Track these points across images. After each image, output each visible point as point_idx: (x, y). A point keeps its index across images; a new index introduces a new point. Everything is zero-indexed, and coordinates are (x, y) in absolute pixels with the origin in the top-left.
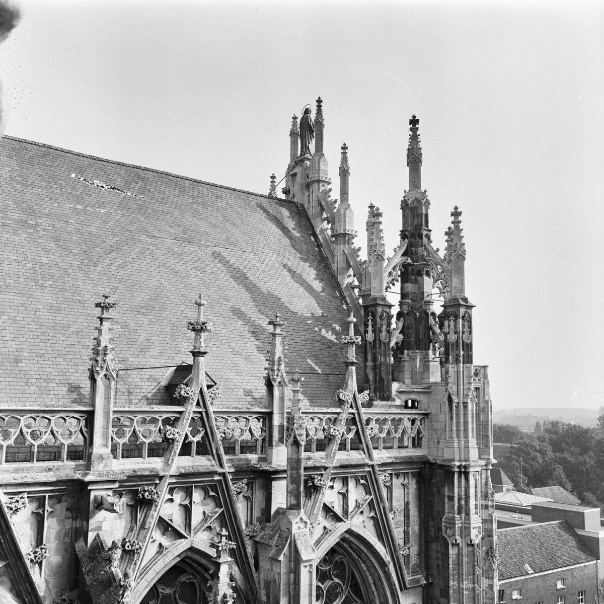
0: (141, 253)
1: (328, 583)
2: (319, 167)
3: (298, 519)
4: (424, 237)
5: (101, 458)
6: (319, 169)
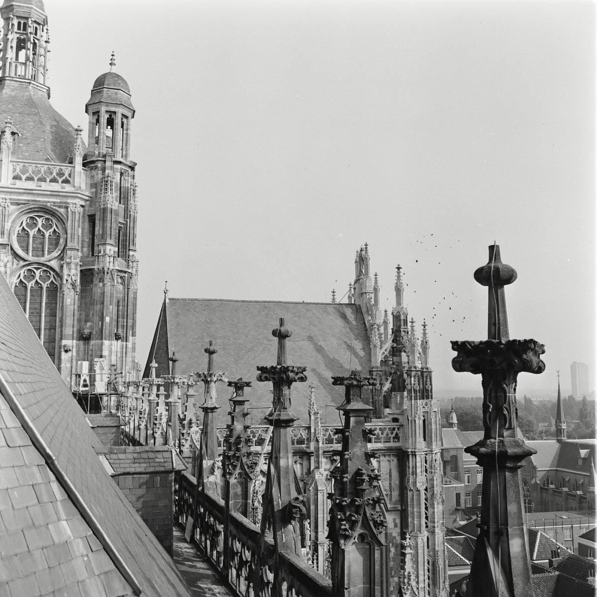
2: (366, 284)
3: (318, 473)
4: (402, 333)
6: (366, 286)
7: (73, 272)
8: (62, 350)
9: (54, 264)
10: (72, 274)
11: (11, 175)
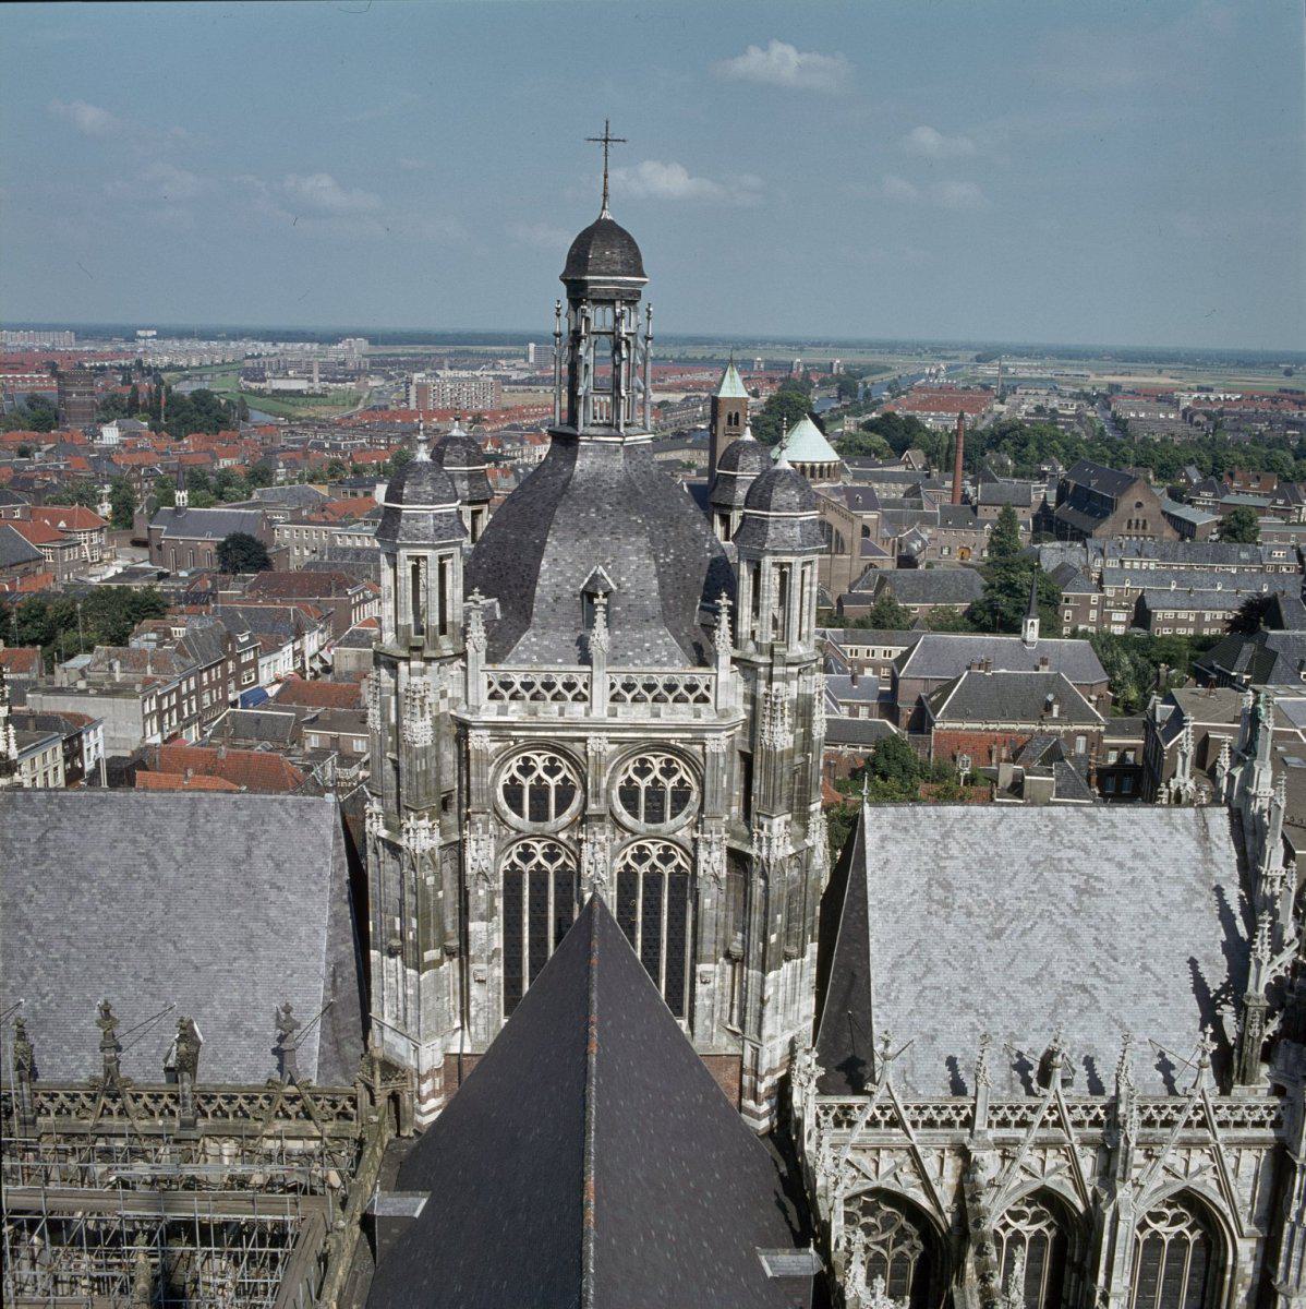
0: (1041, 916)
1: (1175, 1211)
5: (979, 1132)
7: (716, 855)
8: (698, 979)
9: (684, 835)
10: (713, 861)
11: (608, 695)
